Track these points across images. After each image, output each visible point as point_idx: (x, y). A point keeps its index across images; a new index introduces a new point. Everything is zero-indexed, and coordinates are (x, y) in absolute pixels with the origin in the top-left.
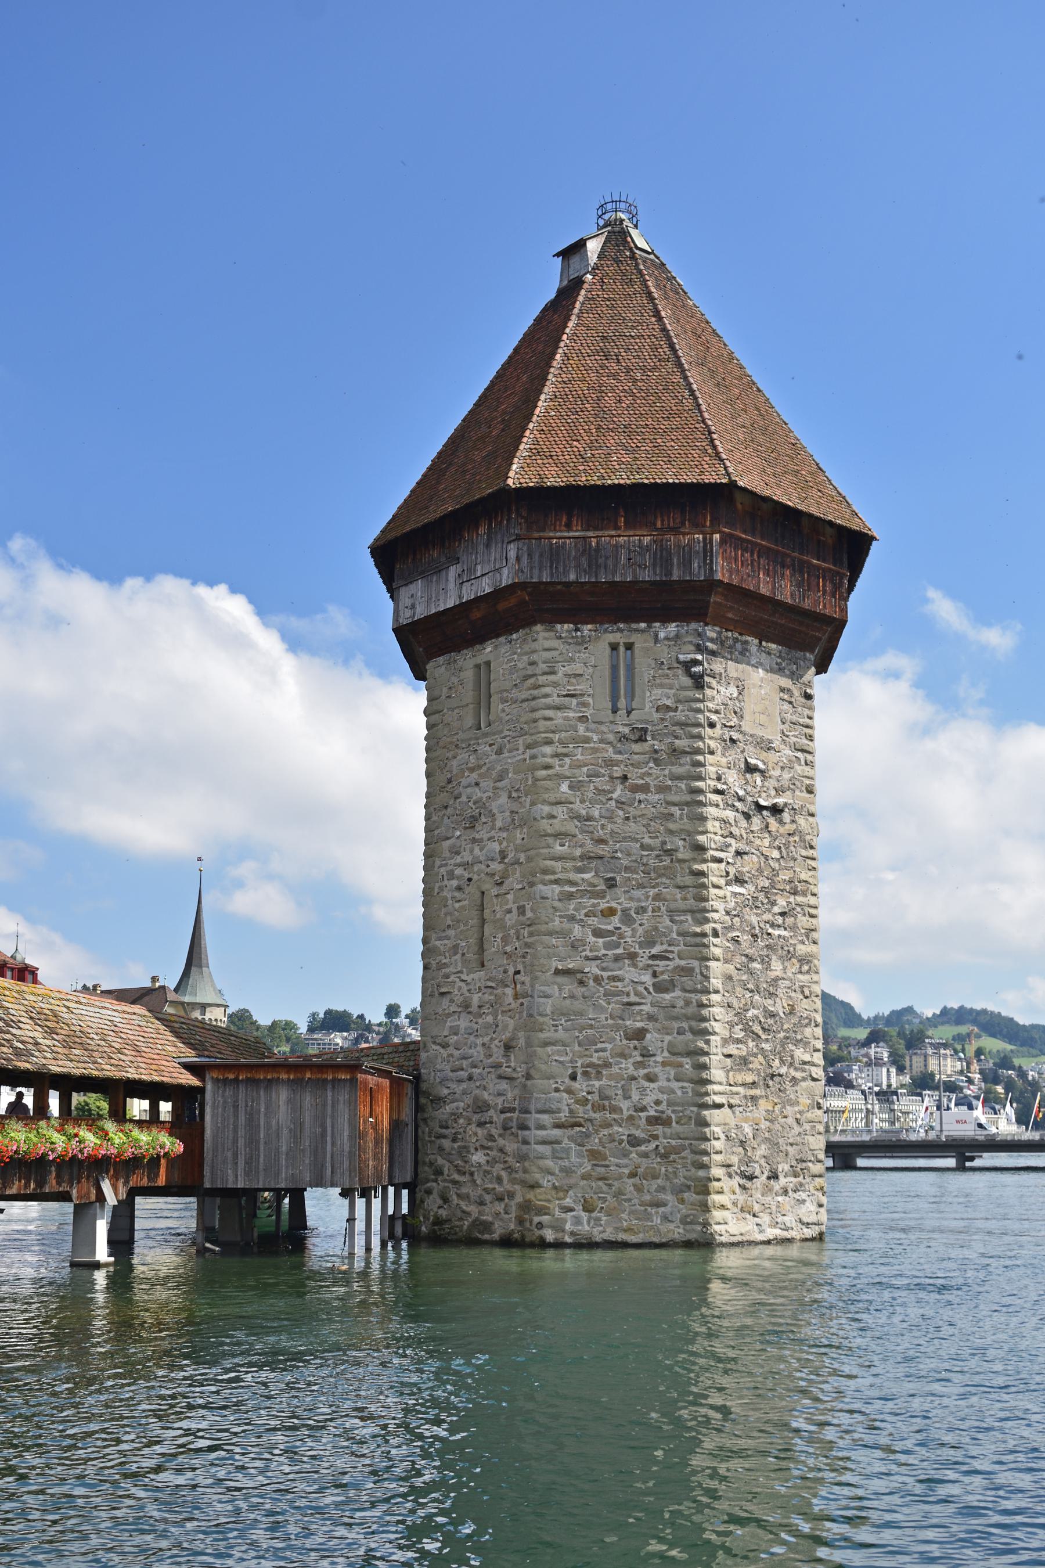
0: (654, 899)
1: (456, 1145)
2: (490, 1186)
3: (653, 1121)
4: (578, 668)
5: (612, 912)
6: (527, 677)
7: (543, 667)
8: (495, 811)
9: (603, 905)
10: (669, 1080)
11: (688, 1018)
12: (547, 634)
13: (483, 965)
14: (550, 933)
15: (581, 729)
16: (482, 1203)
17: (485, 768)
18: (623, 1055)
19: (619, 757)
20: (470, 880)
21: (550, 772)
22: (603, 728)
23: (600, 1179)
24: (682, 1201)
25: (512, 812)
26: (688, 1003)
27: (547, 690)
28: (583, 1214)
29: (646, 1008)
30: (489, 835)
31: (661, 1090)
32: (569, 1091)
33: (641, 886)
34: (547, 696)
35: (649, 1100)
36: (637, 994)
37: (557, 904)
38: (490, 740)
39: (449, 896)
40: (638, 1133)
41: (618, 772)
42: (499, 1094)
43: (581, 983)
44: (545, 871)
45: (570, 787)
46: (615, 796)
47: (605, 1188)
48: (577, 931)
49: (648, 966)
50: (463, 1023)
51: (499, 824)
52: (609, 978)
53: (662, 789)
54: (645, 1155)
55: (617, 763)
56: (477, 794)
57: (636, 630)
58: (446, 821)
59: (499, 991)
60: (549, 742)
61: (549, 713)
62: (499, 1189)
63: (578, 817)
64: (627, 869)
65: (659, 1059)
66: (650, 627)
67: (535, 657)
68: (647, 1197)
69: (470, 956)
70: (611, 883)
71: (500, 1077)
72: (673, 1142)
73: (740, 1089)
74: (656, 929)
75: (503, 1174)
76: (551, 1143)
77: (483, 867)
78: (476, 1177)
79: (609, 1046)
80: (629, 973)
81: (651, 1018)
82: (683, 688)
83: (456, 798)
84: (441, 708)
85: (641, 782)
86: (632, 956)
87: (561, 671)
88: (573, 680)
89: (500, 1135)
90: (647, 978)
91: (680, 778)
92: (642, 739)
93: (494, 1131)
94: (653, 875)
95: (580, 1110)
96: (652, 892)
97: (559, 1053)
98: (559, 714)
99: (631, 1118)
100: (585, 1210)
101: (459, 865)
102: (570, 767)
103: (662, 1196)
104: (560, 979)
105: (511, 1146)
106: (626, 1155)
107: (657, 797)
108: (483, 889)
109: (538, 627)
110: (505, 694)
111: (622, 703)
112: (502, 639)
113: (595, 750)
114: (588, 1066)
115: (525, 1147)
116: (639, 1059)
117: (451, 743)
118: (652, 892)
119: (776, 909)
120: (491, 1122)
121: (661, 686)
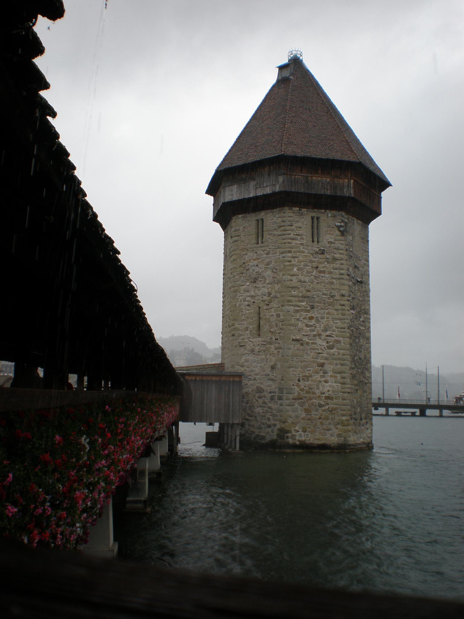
0: (327, 314)
1: (248, 405)
2: (265, 422)
3: (327, 398)
4: (300, 224)
5: (311, 318)
6: (280, 227)
7: (289, 223)
8: (266, 276)
9: (309, 315)
10: (332, 382)
11: (339, 359)
12: (290, 211)
13: (259, 335)
14: (291, 325)
15: (301, 247)
16: (261, 428)
17: (260, 260)
18: (318, 373)
19: (314, 259)
20: (254, 302)
21: (290, 263)
22: (309, 248)
23: (309, 420)
24: (337, 429)
25: (273, 277)
26: (339, 354)
27: (289, 232)
28: (302, 433)
29: (325, 355)
30: (263, 286)
31: (330, 386)
32: (298, 386)
33: (322, 309)
34: (289, 234)
35: (325, 390)
36: (322, 349)
37: (292, 314)
38: (263, 249)
39: (244, 308)
40: (322, 402)
41: (314, 265)
42: (269, 386)
43: (302, 344)
44: (289, 301)
45: (298, 270)
46: (313, 274)
47: (310, 423)
48: (300, 325)
49: (326, 339)
50: (251, 357)
51: (267, 282)
52: (312, 343)
53: (330, 273)
54: (325, 411)
55: (314, 262)
56: (257, 269)
57: (321, 212)
58: (242, 278)
59: (268, 346)
60: (290, 252)
61: (290, 241)
62: (269, 423)
63: (300, 281)
64: (318, 302)
65: (329, 374)
66: (325, 211)
67: (284, 219)
68: (325, 427)
69: (254, 332)
70: (312, 307)
71: (269, 379)
72: (334, 406)
73: (353, 386)
74: (328, 325)
75: (270, 417)
76: (291, 406)
77: (260, 298)
78: (258, 418)
79: (312, 369)
80: (319, 341)
81: (326, 359)
82: (337, 236)
83: (247, 270)
84: (239, 234)
85: (322, 269)
86: (320, 335)
87: (295, 225)
88: (298, 229)
89: (269, 402)
90: (324, 344)
91: (336, 269)
92: (323, 253)
93: (266, 400)
94: (327, 305)
95: (302, 393)
96: (326, 311)
97: (293, 371)
98: (293, 241)
99: (319, 396)
100: (303, 431)
101: (248, 296)
102: (298, 262)
103: (330, 426)
104: (294, 343)
105: (274, 406)
106: (317, 410)
107: (328, 275)
108: (260, 306)
109: (286, 208)
110: (270, 232)
111: (316, 239)
112: (269, 211)
113: (306, 256)
114: (304, 376)
115: (281, 407)
116: (322, 374)
117: (245, 249)
118: (326, 311)
119: (361, 320)
120: (265, 397)
121: (330, 234)
